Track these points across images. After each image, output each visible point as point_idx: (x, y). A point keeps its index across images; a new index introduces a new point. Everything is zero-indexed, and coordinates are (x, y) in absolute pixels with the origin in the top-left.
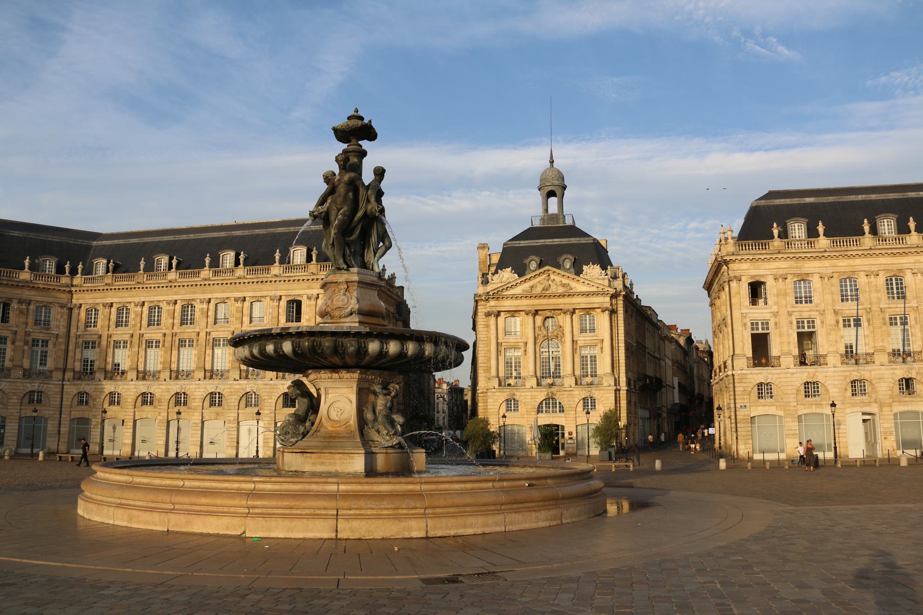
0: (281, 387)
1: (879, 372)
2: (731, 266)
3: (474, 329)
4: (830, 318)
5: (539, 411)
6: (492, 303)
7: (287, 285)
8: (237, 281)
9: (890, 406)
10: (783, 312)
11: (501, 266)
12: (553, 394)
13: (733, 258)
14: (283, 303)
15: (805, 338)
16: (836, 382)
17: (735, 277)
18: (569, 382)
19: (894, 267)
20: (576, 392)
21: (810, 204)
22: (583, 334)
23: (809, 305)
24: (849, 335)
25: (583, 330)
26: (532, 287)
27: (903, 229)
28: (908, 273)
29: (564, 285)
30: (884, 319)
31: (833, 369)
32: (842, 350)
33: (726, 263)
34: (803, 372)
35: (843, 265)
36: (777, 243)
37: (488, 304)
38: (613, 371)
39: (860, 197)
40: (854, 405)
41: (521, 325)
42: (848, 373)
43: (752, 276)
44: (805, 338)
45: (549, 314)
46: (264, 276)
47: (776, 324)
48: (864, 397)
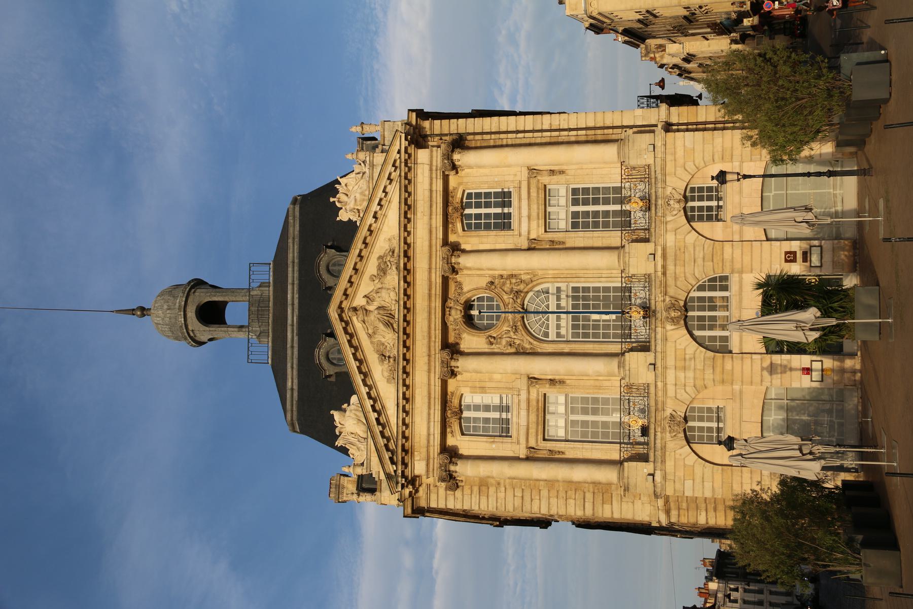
3: (544, 523)
5: (722, 348)
11: (327, 434)
12: (673, 307)
18: (639, 259)
20: (670, 239)
25: (504, 223)
26: (383, 356)
29: (383, 271)
38: (617, 141)
41: (483, 390)
45: (456, 315)
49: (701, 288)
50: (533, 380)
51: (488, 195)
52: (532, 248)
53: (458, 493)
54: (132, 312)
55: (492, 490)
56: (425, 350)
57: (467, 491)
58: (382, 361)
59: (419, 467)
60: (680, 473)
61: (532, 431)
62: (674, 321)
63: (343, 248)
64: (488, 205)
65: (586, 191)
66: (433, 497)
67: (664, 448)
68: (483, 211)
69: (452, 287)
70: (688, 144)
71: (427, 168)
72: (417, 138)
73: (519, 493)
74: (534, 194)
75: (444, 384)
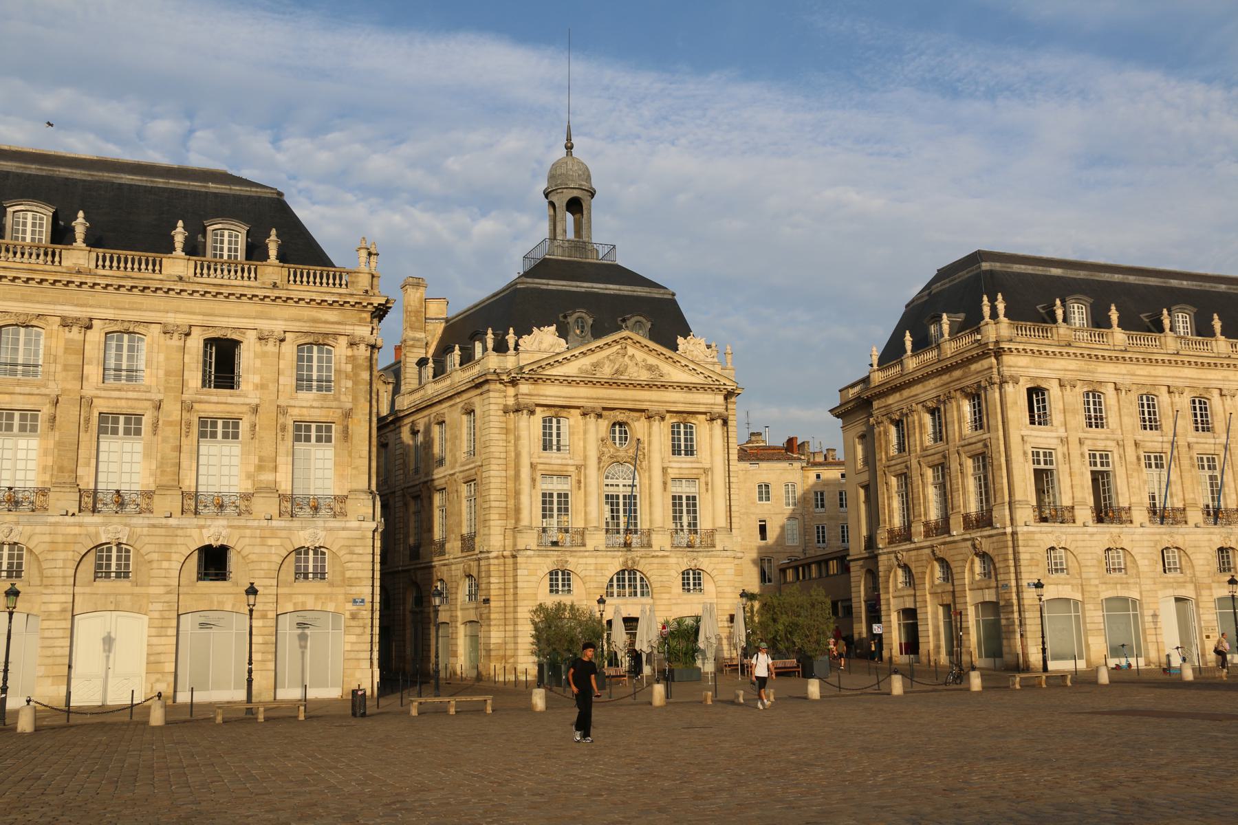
0: (195, 533)
1: (1192, 537)
2: (1006, 359)
4: (1131, 452)
7: (208, 305)
13: (1013, 346)
14: (196, 343)
15: (1100, 481)
19: (1202, 384)
20: (673, 560)
21: (1059, 278)
22: (676, 458)
23: (1099, 430)
24: (1152, 480)
25: (676, 451)
27: (1203, 329)
28: (1216, 393)
29: (650, 368)
30: (1191, 458)
31: (1142, 530)
32: (1147, 502)
34: (1104, 533)
35: (1143, 373)
36: (1063, 329)
37: (511, 391)
39: (1117, 278)
40: (1166, 585)
42: (1158, 537)
43: (1033, 379)
44: (1100, 481)
46: (146, 276)
49: (642, 579)
51: (692, 440)
52: (664, 470)
53: (501, 413)
54: (569, 139)
55: (504, 437)
56: (601, 396)
58: (593, 365)
59: (524, 388)
60: (532, 567)
61: (547, 467)
62: (625, 563)
63: (655, 336)
64: (686, 440)
65: (695, 505)
66: (497, 394)
67: (547, 556)
68: (682, 436)
69: (637, 414)
70: (728, 572)
71: (712, 401)
72: (729, 395)
74: (695, 471)
75: (578, 408)
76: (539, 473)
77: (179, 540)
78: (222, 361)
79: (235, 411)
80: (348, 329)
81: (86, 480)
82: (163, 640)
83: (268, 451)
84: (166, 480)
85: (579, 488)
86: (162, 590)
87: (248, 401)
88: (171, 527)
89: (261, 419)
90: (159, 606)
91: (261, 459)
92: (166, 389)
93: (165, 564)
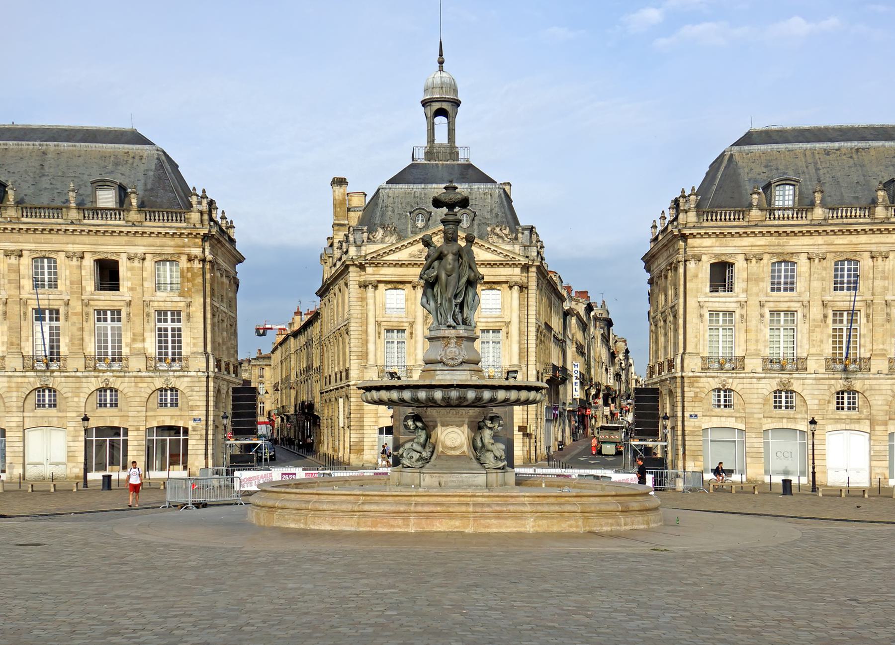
6: (369, 270)
8: (9, 227)
9: (885, 424)
10: (754, 302)
13: (695, 232)
16: (816, 392)
17: (694, 256)
33: (684, 237)
43: (716, 255)
47: (742, 316)
48: (852, 412)
50: (412, 324)
53: (357, 287)
55: (360, 303)
57: (359, 291)
61: (389, 324)
66: (355, 274)
73: (359, 316)
76: (383, 328)
77: (85, 385)
78: (108, 274)
79: (117, 305)
80: (187, 250)
81: (27, 349)
82: (77, 444)
83: (138, 329)
84: (75, 349)
85: (411, 338)
86: (74, 414)
87: (124, 298)
88: (78, 377)
89: (133, 310)
90: (73, 424)
91: (134, 335)
92: (71, 293)
93: (76, 399)
